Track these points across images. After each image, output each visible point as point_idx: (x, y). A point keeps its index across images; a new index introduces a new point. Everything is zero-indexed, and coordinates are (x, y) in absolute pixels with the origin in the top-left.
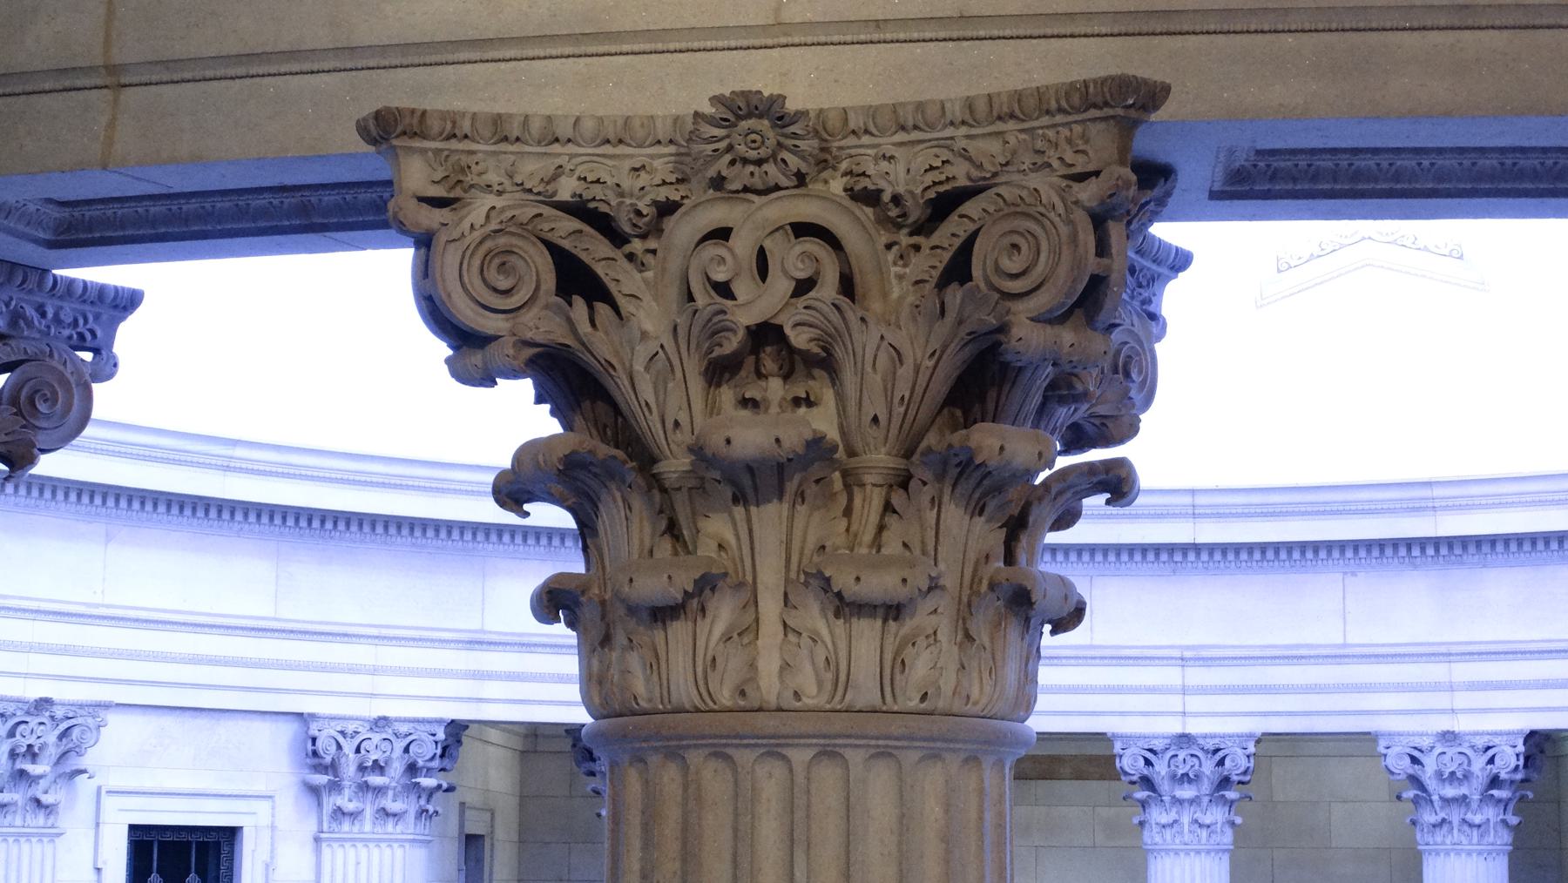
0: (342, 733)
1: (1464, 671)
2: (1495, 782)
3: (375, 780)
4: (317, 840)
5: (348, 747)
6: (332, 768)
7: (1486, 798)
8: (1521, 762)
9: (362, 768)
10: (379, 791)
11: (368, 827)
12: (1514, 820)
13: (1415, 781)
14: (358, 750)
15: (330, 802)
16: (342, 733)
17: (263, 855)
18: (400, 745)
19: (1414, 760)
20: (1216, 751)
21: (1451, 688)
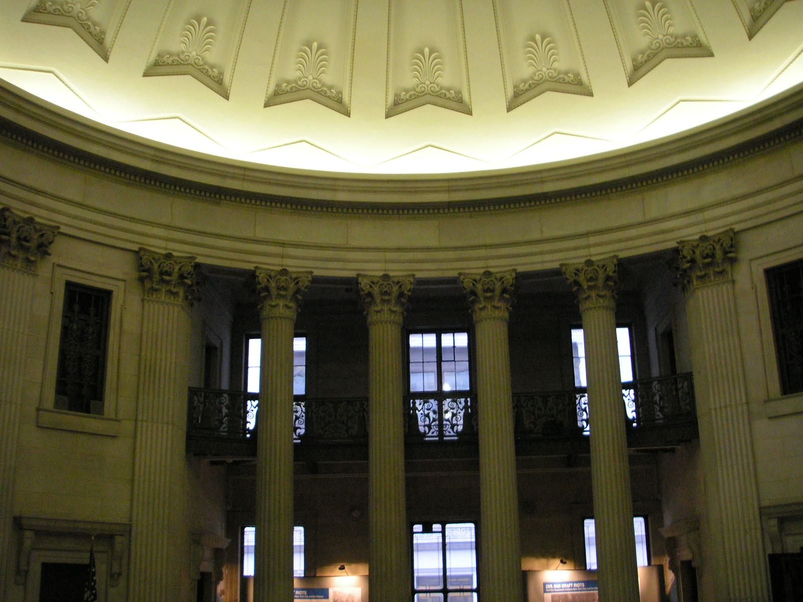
0: (154, 259)
1: (592, 240)
2: (608, 278)
3: (167, 278)
4: (143, 300)
5: (156, 266)
6: (148, 271)
7: (606, 286)
8: (617, 268)
9: (162, 273)
10: (168, 283)
11: (163, 298)
12: (616, 296)
13: (576, 283)
14: (159, 266)
15: (148, 285)
16: (154, 259)
17: (121, 302)
18: (177, 268)
19: (576, 274)
20: (501, 279)
21: (589, 246)
